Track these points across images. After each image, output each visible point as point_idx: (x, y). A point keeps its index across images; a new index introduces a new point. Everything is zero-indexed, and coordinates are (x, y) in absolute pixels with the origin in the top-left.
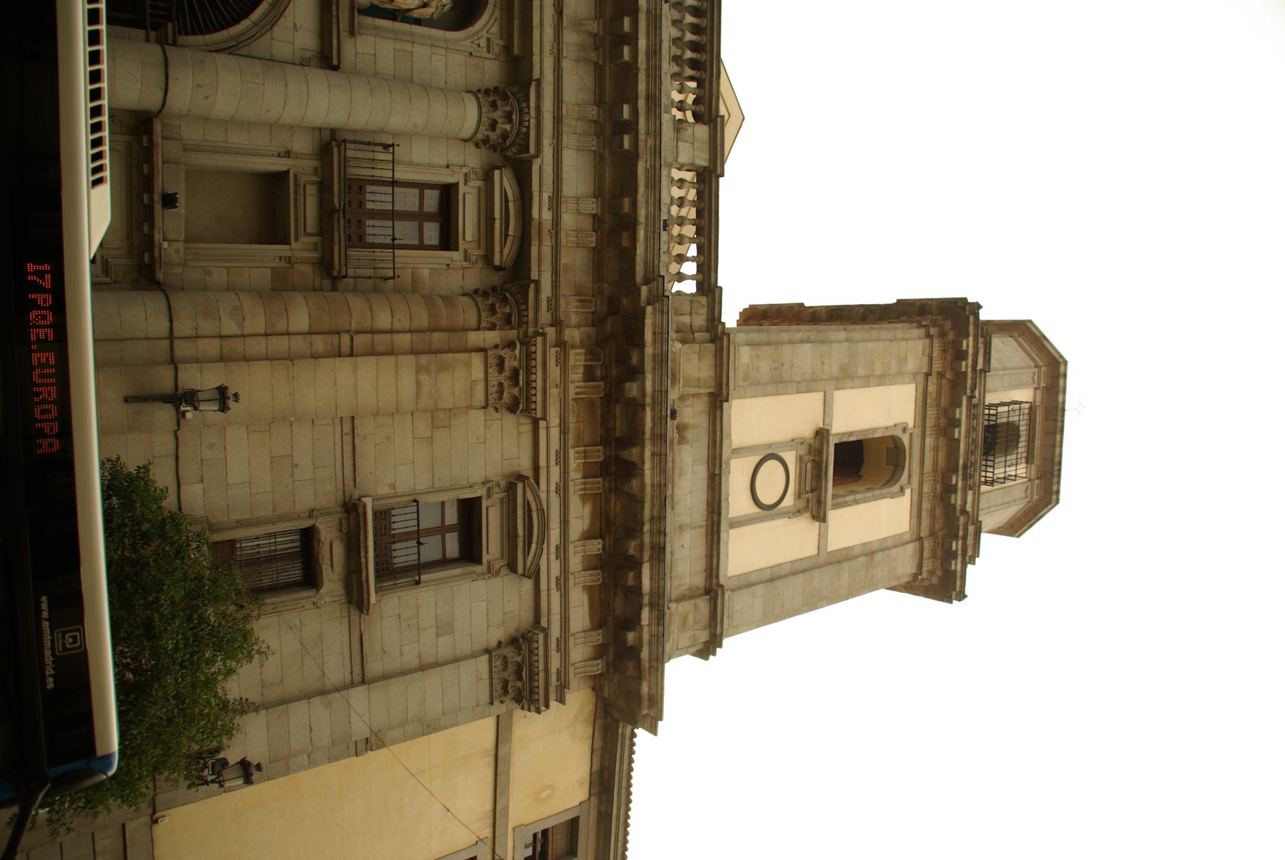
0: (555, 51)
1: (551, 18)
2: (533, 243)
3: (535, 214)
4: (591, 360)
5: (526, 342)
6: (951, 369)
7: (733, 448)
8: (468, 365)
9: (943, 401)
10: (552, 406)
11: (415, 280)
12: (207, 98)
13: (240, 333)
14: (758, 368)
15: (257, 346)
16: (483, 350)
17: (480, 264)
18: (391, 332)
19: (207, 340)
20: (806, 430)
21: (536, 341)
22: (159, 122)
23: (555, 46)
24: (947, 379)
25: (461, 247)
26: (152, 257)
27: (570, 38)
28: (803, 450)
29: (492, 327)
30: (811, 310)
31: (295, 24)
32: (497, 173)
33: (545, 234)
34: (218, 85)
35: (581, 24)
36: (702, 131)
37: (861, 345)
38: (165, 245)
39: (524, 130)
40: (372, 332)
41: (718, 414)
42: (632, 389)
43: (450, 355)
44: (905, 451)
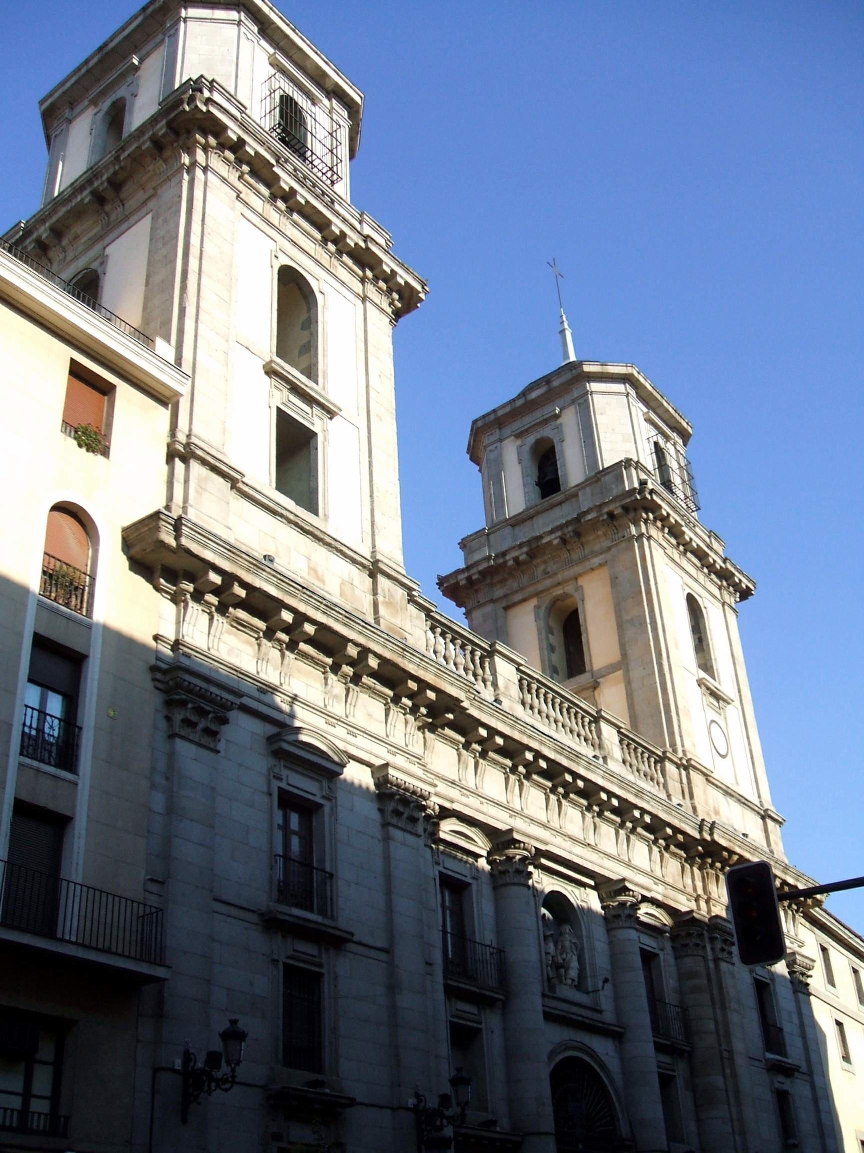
16: (716, 960)
23: (600, 854)
29: (704, 947)
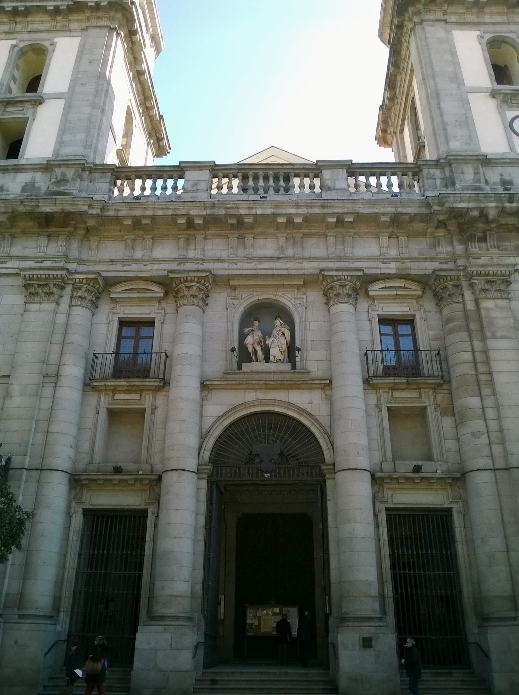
0: (300, 261)
1: (282, 264)
2: (410, 273)
3: (393, 271)
4: (475, 239)
5: (470, 277)
6: (441, 6)
7: (510, 151)
8: (487, 309)
9: (461, 11)
10: (504, 262)
11: (436, 338)
12: (363, 449)
13: (486, 434)
14: (462, 136)
15: (493, 425)
16: (477, 302)
17: (421, 302)
18: (473, 352)
19: (493, 451)
20: (492, 104)
21: (471, 271)
22: (376, 473)
23: (298, 261)
24: (447, 9)
25: (413, 313)
26: (448, 478)
27: (290, 252)
28: (505, 106)
30: (386, 101)
31: (309, 403)
32: (371, 293)
33: (403, 266)
34: (356, 443)
35: (282, 247)
36: (327, 174)
37: (437, 69)
38: (438, 471)
39: (349, 278)
40: (475, 363)
41: (493, 161)
42: (492, 214)
43: (484, 320)
44: (494, 36)
